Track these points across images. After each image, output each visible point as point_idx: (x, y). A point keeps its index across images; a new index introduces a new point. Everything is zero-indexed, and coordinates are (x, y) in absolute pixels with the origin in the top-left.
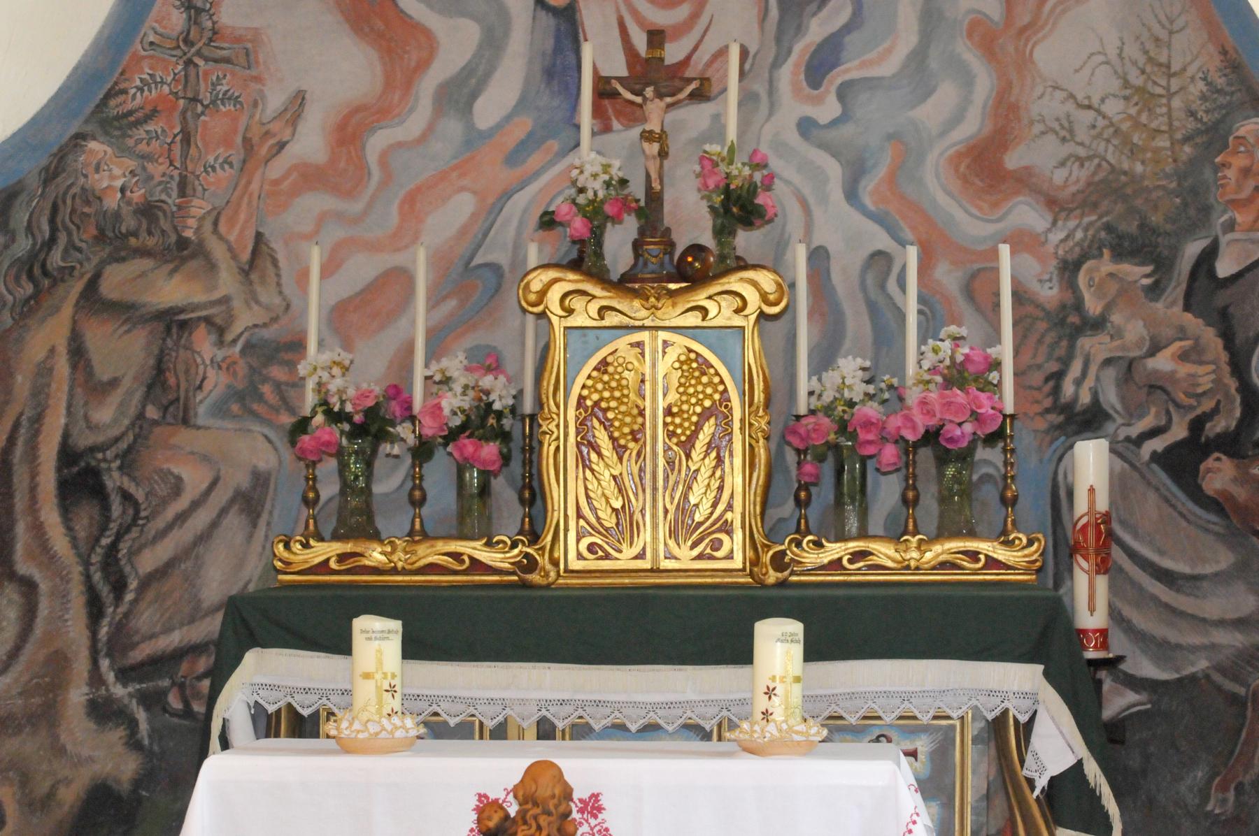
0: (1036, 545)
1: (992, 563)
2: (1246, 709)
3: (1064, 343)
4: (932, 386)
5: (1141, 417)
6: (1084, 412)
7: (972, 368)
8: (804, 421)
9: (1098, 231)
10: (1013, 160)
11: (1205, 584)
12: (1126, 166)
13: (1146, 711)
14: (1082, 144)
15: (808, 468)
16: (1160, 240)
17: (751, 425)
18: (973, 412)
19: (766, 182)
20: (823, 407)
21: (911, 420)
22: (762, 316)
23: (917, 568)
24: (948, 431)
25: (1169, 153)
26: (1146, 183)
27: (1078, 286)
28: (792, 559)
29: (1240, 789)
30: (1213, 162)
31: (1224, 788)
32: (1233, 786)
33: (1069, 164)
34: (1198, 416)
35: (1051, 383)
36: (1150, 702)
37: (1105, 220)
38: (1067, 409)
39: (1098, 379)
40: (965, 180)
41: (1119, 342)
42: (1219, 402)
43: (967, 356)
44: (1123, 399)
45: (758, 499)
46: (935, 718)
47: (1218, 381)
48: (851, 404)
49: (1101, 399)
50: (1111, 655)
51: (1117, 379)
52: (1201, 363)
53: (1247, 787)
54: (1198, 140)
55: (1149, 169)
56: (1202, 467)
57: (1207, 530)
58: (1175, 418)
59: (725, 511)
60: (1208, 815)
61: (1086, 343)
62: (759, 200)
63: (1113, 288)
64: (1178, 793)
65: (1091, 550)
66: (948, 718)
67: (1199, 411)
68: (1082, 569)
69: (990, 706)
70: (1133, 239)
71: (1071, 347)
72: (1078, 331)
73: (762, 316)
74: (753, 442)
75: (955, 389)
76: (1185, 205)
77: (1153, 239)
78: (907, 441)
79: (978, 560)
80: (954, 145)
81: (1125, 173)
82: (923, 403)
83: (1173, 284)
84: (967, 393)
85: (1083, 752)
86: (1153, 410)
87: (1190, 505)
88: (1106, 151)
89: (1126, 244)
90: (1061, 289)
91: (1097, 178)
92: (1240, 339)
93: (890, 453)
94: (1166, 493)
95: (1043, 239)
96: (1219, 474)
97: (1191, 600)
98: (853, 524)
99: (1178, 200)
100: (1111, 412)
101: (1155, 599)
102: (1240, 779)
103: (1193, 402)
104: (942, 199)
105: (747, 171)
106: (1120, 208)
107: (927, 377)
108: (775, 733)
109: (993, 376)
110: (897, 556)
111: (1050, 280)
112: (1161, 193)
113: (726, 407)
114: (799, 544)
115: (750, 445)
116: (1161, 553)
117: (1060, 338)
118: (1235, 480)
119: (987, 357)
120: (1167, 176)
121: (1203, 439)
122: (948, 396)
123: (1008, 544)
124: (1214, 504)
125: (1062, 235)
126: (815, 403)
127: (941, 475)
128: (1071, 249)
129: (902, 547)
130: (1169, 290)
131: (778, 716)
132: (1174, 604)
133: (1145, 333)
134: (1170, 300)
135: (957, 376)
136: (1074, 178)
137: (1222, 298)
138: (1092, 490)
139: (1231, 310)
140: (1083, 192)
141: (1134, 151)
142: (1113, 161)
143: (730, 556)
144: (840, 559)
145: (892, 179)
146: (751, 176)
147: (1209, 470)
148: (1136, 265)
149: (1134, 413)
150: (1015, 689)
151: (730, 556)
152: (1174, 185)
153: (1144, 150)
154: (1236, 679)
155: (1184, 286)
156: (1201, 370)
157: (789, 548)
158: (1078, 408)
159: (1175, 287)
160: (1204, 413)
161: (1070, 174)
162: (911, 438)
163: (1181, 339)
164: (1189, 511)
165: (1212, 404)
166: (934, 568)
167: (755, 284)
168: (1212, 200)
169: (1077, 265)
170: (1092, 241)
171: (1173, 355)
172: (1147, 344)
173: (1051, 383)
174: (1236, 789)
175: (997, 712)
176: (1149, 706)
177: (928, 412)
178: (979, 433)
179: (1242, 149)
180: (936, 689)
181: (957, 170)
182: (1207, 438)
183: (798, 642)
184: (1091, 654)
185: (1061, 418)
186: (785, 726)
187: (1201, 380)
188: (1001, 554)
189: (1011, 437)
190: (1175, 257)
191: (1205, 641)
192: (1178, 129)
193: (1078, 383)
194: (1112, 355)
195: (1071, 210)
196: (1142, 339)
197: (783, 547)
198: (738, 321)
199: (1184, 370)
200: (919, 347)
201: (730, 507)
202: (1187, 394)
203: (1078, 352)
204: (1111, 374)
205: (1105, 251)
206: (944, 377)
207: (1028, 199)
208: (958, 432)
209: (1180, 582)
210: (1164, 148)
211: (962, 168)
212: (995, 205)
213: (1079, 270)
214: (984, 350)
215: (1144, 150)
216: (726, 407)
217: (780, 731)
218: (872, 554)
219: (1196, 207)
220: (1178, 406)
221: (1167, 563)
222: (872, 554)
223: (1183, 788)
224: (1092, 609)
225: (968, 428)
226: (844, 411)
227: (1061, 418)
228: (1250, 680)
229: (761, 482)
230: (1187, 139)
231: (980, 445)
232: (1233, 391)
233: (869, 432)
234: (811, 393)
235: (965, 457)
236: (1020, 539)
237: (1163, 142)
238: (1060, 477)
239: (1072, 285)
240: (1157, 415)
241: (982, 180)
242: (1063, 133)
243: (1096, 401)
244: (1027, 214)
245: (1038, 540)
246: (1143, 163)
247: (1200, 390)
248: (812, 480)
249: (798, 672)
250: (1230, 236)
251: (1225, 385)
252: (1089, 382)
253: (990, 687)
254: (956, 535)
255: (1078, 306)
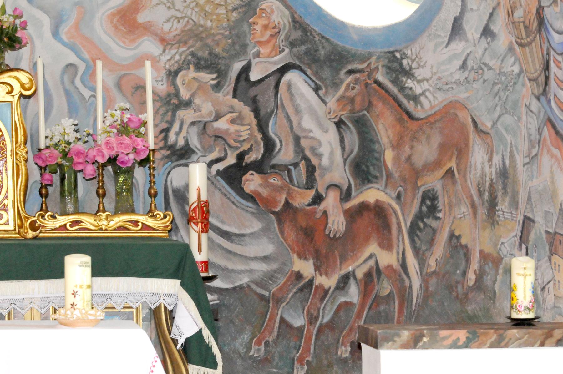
0: (168, 217)
1: (146, 227)
2: (269, 302)
3: (170, 114)
4: (111, 134)
5: (211, 152)
6: (181, 149)
7: (132, 125)
8: (43, 152)
9: (187, 56)
10: (142, 18)
11: (246, 239)
12: (202, 22)
13: (217, 304)
14: (179, 10)
15: (47, 176)
16: (220, 61)
17: (17, 154)
18: (134, 148)
19: (22, 25)
20: (53, 144)
21: (102, 152)
22: (22, 95)
23: (106, 230)
24: (121, 158)
25: (225, 16)
26: (213, 31)
27: (177, 84)
28: (40, 225)
29: (267, 344)
30: (248, 22)
31: (259, 343)
32: (263, 342)
33: (172, 20)
34: (241, 152)
35: (163, 135)
36: (219, 299)
37: (191, 50)
38: (172, 148)
39: (188, 132)
40: (116, 28)
41: (199, 113)
42: (252, 145)
43: (129, 119)
44: (201, 143)
45: (22, 193)
46: (124, 308)
47: (251, 134)
48: (69, 143)
49: (190, 143)
50: (210, 275)
51: (198, 132)
52: (243, 125)
53: (271, 343)
54: (240, 10)
55: (214, 24)
56: (244, 178)
57: (247, 211)
58: (229, 152)
59: (4, 199)
60: (251, 357)
61: (180, 113)
62: (18, 35)
63: (196, 85)
64: (235, 346)
65: (199, 221)
66: (131, 308)
67: (241, 150)
68: (194, 230)
69: (153, 301)
70: (206, 60)
71: (174, 115)
72: (177, 107)
73: (22, 95)
74: (18, 163)
75: (124, 136)
76: (234, 43)
77: (216, 60)
78: (98, 163)
79: (138, 226)
80: (110, 9)
81: (202, 26)
82: (107, 143)
83: (227, 83)
84: (131, 138)
85: (202, 325)
86: (217, 149)
87: (238, 198)
88: (192, 14)
89: (202, 63)
90: (168, 86)
91: (186, 28)
92: (262, 113)
93: (90, 169)
94: (225, 192)
95: (158, 59)
96: (252, 182)
97: (239, 247)
98: (70, 207)
99: (230, 41)
100: (195, 149)
101: (220, 246)
102: (267, 339)
103: (238, 145)
104: (105, 38)
105: (11, 19)
106: (198, 44)
107: (109, 129)
108: (79, 315)
109: (142, 130)
110: (96, 223)
111: (162, 81)
112: (220, 37)
113: (3, 144)
114: (43, 217)
115: (17, 164)
116: (222, 222)
117: (168, 111)
118: (261, 185)
119: (140, 120)
120: (224, 28)
121: (244, 164)
122: (121, 140)
123: (154, 217)
124: (251, 198)
125: (168, 57)
126: (48, 143)
127: (117, 181)
128: (173, 65)
129: (98, 218)
130: (225, 87)
131: (79, 305)
132: (230, 249)
133: (212, 109)
134: (226, 92)
135: (124, 129)
136: (174, 28)
137: (253, 92)
138: (199, 189)
139: (258, 98)
140: (179, 35)
141: (206, 15)
142: (195, 20)
143: (7, 223)
144: (65, 225)
145: (77, 26)
146: (14, 22)
147: (247, 180)
148: (208, 73)
149: (207, 150)
150: (166, 292)
151: (7, 223)
152: (227, 33)
153: (211, 14)
154: (263, 288)
155: (233, 85)
156: (242, 128)
157: (38, 219)
158: (178, 147)
159: (228, 86)
160: (244, 150)
161: (172, 26)
162: (101, 161)
163: (232, 112)
164: (237, 201)
165: (248, 146)
166: (115, 230)
167: (17, 79)
168: (248, 41)
169: (176, 73)
170: (184, 61)
171: (227, 120)
172: (214, 114)
173: (163, 135)
174: (265, 343)
175: (157, 305)
176: (218, 302)
177: (110, 147)
178: (137, 159)
179: (264, 15)
180: (125, 293)
181: (112, 22)
182: (246, 163)
183: (88, 266)
184: (203, 275)
185: (169, 152)
186: (84, 311)
187: (242, 134)
188: (150, 222)
189: (154, 162)
190: (228, 70)
191: (247, 268)
192: (230, 4)
193: (178, 134)
194: (195, 120)
195: (173, 45)
196: (211, 112)
197: (36, 218)
198: (9, 98)
199: (233, 128)
200: (103, 114)
201: (6, 197)
202: (235, 141)
203: (177, 118)
204: (194, 130)
205: (191, 66)
206: (117, 129)
207: (150, 38)
208: (126, 158)
209: (233, 238)
210: (223, 14)
211: (115, 21)
212: (133, 41)
213: (177, 76)
214: (138, 116)
215: (211, 14)
216: (3, 144)
217: (82, 314)
218: (82, 222)
219: (239, 45)
220: (230, 146)
221: (225, 228)
222: (82, 222)
223: (237, 344)
224: (200, 251)
225: (131, 156)
226: (65, 147)
227: (169, 152)
228: (271, 288)
229: (23, 184)
230: (235, 9)
231: (137, 166)
232: (259, 139)
233: (79, 158)
234: (47, 137)
235: (129, 171)
236: (160, 215)
237: (222, 10)
238: (169, 183)
239: (174, 84)
240: (220, 151)
241: (125, 28)
242: (168, 4)
243: (187, 144)
244: (149, 46)
245: (169, 215)
246: (211, 21)
247: (242, 139)
248: (49, 183)
249: (89, 283)
250: (257, 60)
251: (256, 136)
252: (183, 134)
253: (153, 292)
254: (126, 212)
255: (177, 94)
